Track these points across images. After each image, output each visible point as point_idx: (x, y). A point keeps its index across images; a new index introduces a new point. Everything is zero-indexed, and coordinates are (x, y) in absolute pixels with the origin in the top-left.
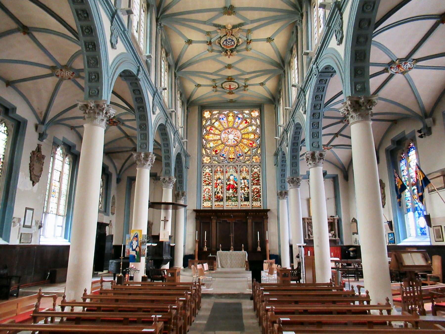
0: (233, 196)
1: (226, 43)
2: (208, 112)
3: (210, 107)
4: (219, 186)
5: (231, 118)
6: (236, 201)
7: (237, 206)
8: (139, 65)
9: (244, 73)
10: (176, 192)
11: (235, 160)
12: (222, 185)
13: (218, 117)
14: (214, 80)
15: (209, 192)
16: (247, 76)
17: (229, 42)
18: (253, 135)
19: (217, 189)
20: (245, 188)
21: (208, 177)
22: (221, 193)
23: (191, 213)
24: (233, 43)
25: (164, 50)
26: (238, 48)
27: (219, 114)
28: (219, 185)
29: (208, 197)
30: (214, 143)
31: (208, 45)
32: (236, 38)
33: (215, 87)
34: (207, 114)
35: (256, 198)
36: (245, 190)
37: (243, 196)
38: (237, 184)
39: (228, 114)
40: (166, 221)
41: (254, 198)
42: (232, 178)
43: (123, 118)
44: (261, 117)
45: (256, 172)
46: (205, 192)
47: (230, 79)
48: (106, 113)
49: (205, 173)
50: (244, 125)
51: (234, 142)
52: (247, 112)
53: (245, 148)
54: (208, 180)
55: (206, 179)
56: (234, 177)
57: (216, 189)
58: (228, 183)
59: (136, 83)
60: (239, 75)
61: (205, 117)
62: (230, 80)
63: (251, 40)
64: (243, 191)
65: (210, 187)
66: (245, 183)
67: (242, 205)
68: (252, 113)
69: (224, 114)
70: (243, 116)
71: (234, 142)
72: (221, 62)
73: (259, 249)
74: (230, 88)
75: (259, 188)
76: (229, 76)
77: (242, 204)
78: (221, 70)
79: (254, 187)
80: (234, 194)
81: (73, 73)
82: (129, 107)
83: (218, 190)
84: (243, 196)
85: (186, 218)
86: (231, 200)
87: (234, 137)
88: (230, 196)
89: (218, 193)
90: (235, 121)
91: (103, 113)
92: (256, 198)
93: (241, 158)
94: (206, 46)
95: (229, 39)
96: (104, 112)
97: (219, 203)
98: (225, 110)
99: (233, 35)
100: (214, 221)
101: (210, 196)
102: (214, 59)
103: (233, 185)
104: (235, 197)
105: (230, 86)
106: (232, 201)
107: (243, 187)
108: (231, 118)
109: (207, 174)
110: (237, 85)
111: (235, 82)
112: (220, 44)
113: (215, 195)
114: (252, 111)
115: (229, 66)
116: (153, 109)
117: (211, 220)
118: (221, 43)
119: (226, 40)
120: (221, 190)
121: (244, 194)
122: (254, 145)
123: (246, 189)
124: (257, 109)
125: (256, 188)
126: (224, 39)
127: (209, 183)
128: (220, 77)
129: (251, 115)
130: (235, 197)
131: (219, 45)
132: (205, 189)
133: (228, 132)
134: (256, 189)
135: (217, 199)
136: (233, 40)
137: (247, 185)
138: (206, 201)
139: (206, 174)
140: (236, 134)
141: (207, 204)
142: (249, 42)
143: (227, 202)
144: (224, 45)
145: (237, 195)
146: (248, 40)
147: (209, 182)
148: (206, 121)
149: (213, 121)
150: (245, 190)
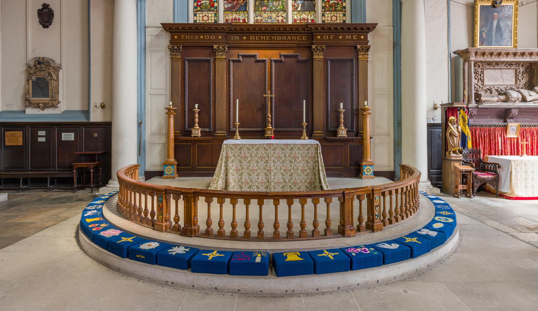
23: (158, 36)
73: (343, 132)
85: (143, 50)
86: (267, 6)
97: (237, 16)
100: (221, 56)
117: (214, 52)
135: (230, 5)
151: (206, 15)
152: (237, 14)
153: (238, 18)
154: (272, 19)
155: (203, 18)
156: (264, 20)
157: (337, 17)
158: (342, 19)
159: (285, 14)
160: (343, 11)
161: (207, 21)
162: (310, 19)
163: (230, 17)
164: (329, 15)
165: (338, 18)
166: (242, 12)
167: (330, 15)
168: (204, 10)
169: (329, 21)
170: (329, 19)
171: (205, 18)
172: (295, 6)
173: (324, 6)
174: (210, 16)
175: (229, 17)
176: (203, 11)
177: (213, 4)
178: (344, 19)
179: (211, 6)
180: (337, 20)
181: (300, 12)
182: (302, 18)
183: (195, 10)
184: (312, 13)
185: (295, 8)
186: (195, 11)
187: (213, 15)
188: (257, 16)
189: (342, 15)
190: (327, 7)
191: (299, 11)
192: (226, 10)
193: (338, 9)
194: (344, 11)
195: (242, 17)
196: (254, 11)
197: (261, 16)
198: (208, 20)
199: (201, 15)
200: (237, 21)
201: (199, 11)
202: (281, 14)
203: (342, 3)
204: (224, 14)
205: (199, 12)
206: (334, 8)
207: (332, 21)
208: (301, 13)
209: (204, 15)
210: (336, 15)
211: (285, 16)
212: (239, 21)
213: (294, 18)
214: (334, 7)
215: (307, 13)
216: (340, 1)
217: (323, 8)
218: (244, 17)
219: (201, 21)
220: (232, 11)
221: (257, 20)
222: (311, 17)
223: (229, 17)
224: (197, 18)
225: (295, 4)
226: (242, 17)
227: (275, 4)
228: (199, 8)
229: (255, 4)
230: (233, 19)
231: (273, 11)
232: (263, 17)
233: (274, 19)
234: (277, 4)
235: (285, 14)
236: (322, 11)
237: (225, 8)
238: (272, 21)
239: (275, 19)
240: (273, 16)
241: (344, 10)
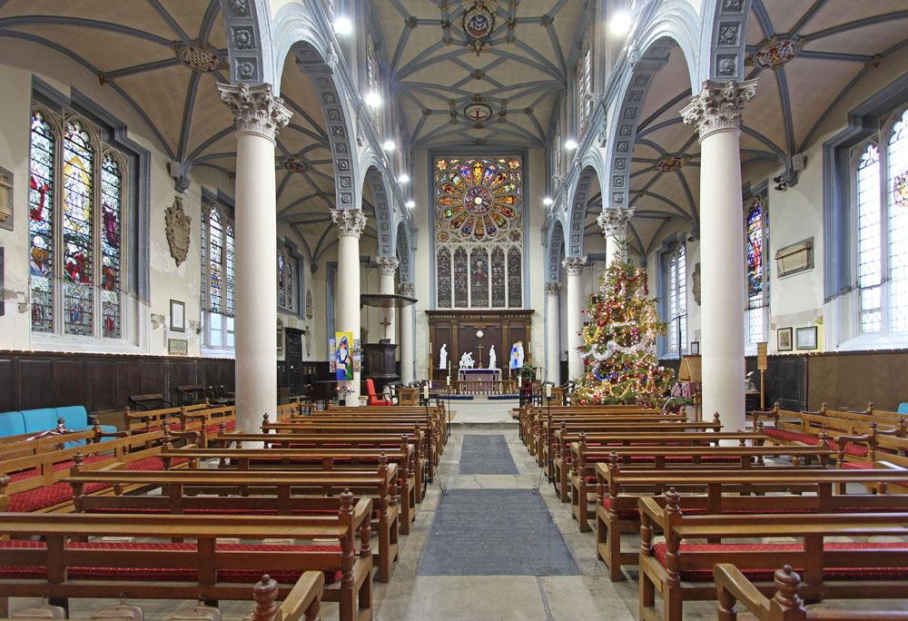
1: (474, 24)
3: (447, 153)
5: (477, 171)
8: (328, 40)
9: (502, 88)
10: (399, 285)
11: (484, 238)
13: (459, 168)
14: (452, 102)
16: (505, 95)
17: (479, 23)
18: (511, 199)
24: (485, 26)
25: (370, 36)
26: (493, 38)
31: (444, 27)
32: (492, 14)
33: (454, 114)
34: (441, 165)
39: (473, 163)
40: (386, 323)
42: (479, 263)
43: (310, 156)
44: (524, 169)
47: (478, 99)
48: (274, 114)
50: (498, 182)
52: (502, 161)
59: (326, 79)
60: (493, 92)
62: (477, 102)
63: (515, 20)
65: (447, 278)
66: (498, 272)
68: (510, 163)
69: (468, 165)
70: (497, 168)
72: (465, 66)
74: (478, 118)
76: (477, 95)
78: (464, 82)
79: (512, 277)
81: (214, 57)
82: (317, 129)
89: (460, 286)
90: (484, 175)
91: (268, 112)
94: (438, 32)
95: (480, 16)
96: (271, 111)
98: (469, 158)
99: (486, 8)
102: (453, 57)
105: (478, 112)
108: (477, 171)
110: (488, 110)
111: (485, 105)
112: (463, 26)
113: (455, 289)
114: (511, 160)
115: (478, 75)
116: (357, 135)
118: (466, 25)
119: (474, 19)
122: (512, 214)
124: (517, 157)
126: (470, 16)
128: (461, 96)
129: (509, 166)
131: (462, 30)
133: (474, 193)
136: (485, 20)
142: (512, 24)
144: (470, 29)
146: (510, 19)
149: (452, 176)
192: (456, 299)
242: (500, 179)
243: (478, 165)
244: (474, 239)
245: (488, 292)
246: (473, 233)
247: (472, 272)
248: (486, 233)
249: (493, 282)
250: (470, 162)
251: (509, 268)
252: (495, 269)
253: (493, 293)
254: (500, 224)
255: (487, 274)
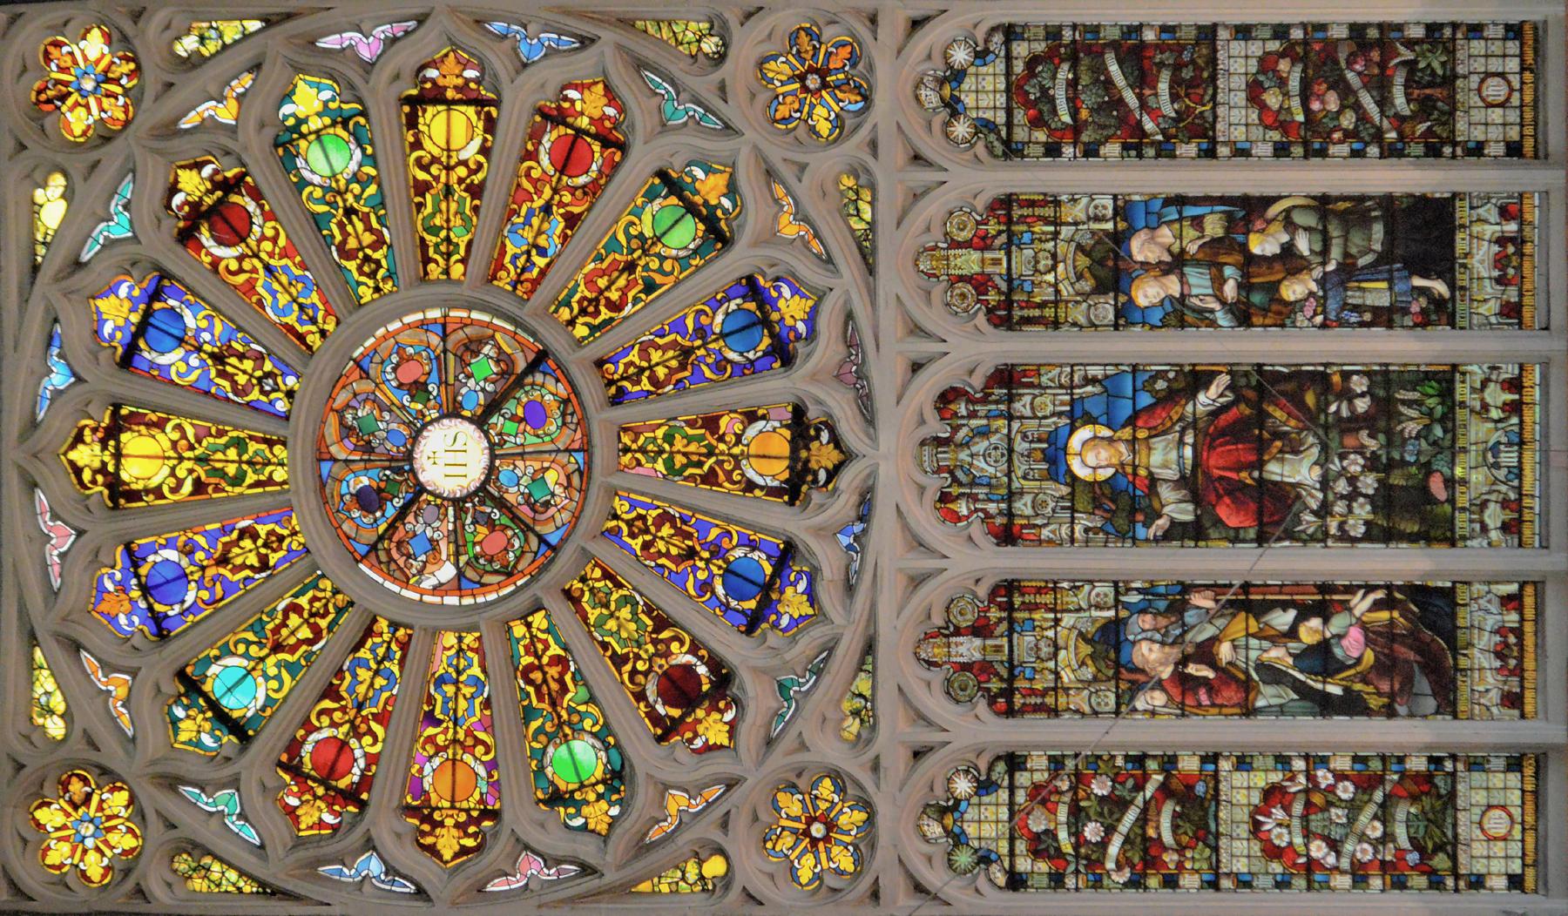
0: (1372, 445)
2: (50, 817)
4: (1225, 652)
6: (1447, 394)
7: (1515, 385)
11: (840, 406)
12: (1202, 601)
15: (1316, 802)
18: (434, 122)
19: (1272, 674)
20: (1249, 261)
21: (1077, 815)
22: (1323, 611)
27: (76, 647)
28: (1205, 653)
29: (1384, 815)
30: (563, 730)
35: (1399, 100)
36: (1289, 260)
37: (1377, 293)
38: (1198, 379)
41: (1400, 120)
45: (1014, 90)
46: (1318, 850)
49: (1023, 865)
51: (534, 416)
52: (52, 208)
53: (645, 244)
54: (1131, 816)
55: (1114, 849)
56: (1077, 416)
57: (1268, 696)
58: (1176, 507)
61: (125, 868)
64: (1293, 290)
66: (1177, 263)
67: (1512, 312)
68: (78, 121)
70: (130, 262)
71: (534, 416)
75: (1256, 48)
77: (1492, 307)
80: (1355, 423)
83: (1278, 655)
84: (1377, 293)
87: (453, 411)
88: (1369, 483)
89: (1322, 658)
92: (1399, 100)
93: (792, 308)
101: (1366, 783)
103: (1213, 431)
104: (1383, 415)
106: (1453, 452)
107: (1230, 290)
109: (1038, 823)
113: (1351, 705)
120: (1282, 619)
121: (1348, 272)
122: (590, 106)
123: (1263, 244)
125: (1254, 92)
127: (1178, 791)
129: (104, 136)
130: (1383, 415)
132: (1273, 852)
133: (368, 500)
134: (1273, 99)
135: (1423, 684)
137: (1214, 226)
138: (1450, 846)
139: (1041, 845)
140: (417, 389)
141: (1497, 823)
143: (1461, 520)
145: (1359, 384)
147: (1165, 791)
148: (197, 848)
150: (1289, 260)
151: (1476, 818)
152: (1470, 645)
153: (1498, 638)
154: (1499, 443)
155: (1496, 839)
156: (1503, 488)
157: (1488, 75)
158: (1499, 43)
159: (1469, 368)
160: (1454, 39)
161: (1510, 815)
162: (1498, 228)
163: (1490, 678)
164: (1474, 119)
165: (1495, 65)
166: (1461, 612)
167: (1473, 112)
168: (1450, 834)
169: (1513, 116)
170: (1496, 115)
171: (1497, 823)
172: (1423, 311)
173: (1427, 145)
174: (1480, 798)
175: (1487, 691)
176: (1456, 836)
177: (1417, 777)
178: (1500, 32)
179: (1427, 794)
180: (1502, 75)
181: (1459, 283)
182: (1496, 273)
183: (1450, 882)
184: (1462, 213)
185: (1436, 312)
186: (1456, 885)
187: (1477, 777)
188: (1485, 529)
189: (1474, 43)
190: (1429, 128)
191: (1452, 286)
192: (1448, 704)
193: (1443, 64)
194: (1454, 33)
195: (1488, 612)
196: (1453, 545)
197: (1483, 505)
198: (1503, 808)
199: (1479, 849)
200: (1512, 639)
201: (1454, 858)
202: (1473, 390)
203: (1410, 44)
204: (1471, 718)
205: (1462, 858)
206: (1437, 92)
207: (1508, 100)
208: (1462, 279)
209: (1478, 832)
210: (1475, 79)
211: (1485, 367)
212: (1512, 630)
213: (1493, 320)
214: (1428, 91)
215: (1461, 244)
216: (1399, 54)
217: (1433, 151)
218: (1489, 601)
219: (1515, 849)
220: (1456, 668)
221: (1505, 528)
222: (1486, 221)
223: (1487, 691)
224: (1494, 869)
225: (1415, 308)
226: (1488, 612)
227: (1412, 428)
228: (1441, 861)
229: (1412, 538)
230: (1498, 664)
231: (1454, 440)
232: (1489, 493)
233: (1497, 429)
234: (1413, 413)
235: (1469, 368)
236: (1454, 156)
237: (1437, 712)
238: (1509, 444)
239: (1500, 425)
240: (1481, 436)
241: (1447, 32)
242: (234, 230)
243: (87, 455)
244: (843, 504)
245: (1384, 379)
246: (781, 519)
247: (1177, 533)
248: (776, 388)
249: (1283, 314)
250: (61, 539)
251: (1135, 144)
252: (1147, 293)
253: (1384, 318)
254: (686, 233)
255: (1198, 379)
